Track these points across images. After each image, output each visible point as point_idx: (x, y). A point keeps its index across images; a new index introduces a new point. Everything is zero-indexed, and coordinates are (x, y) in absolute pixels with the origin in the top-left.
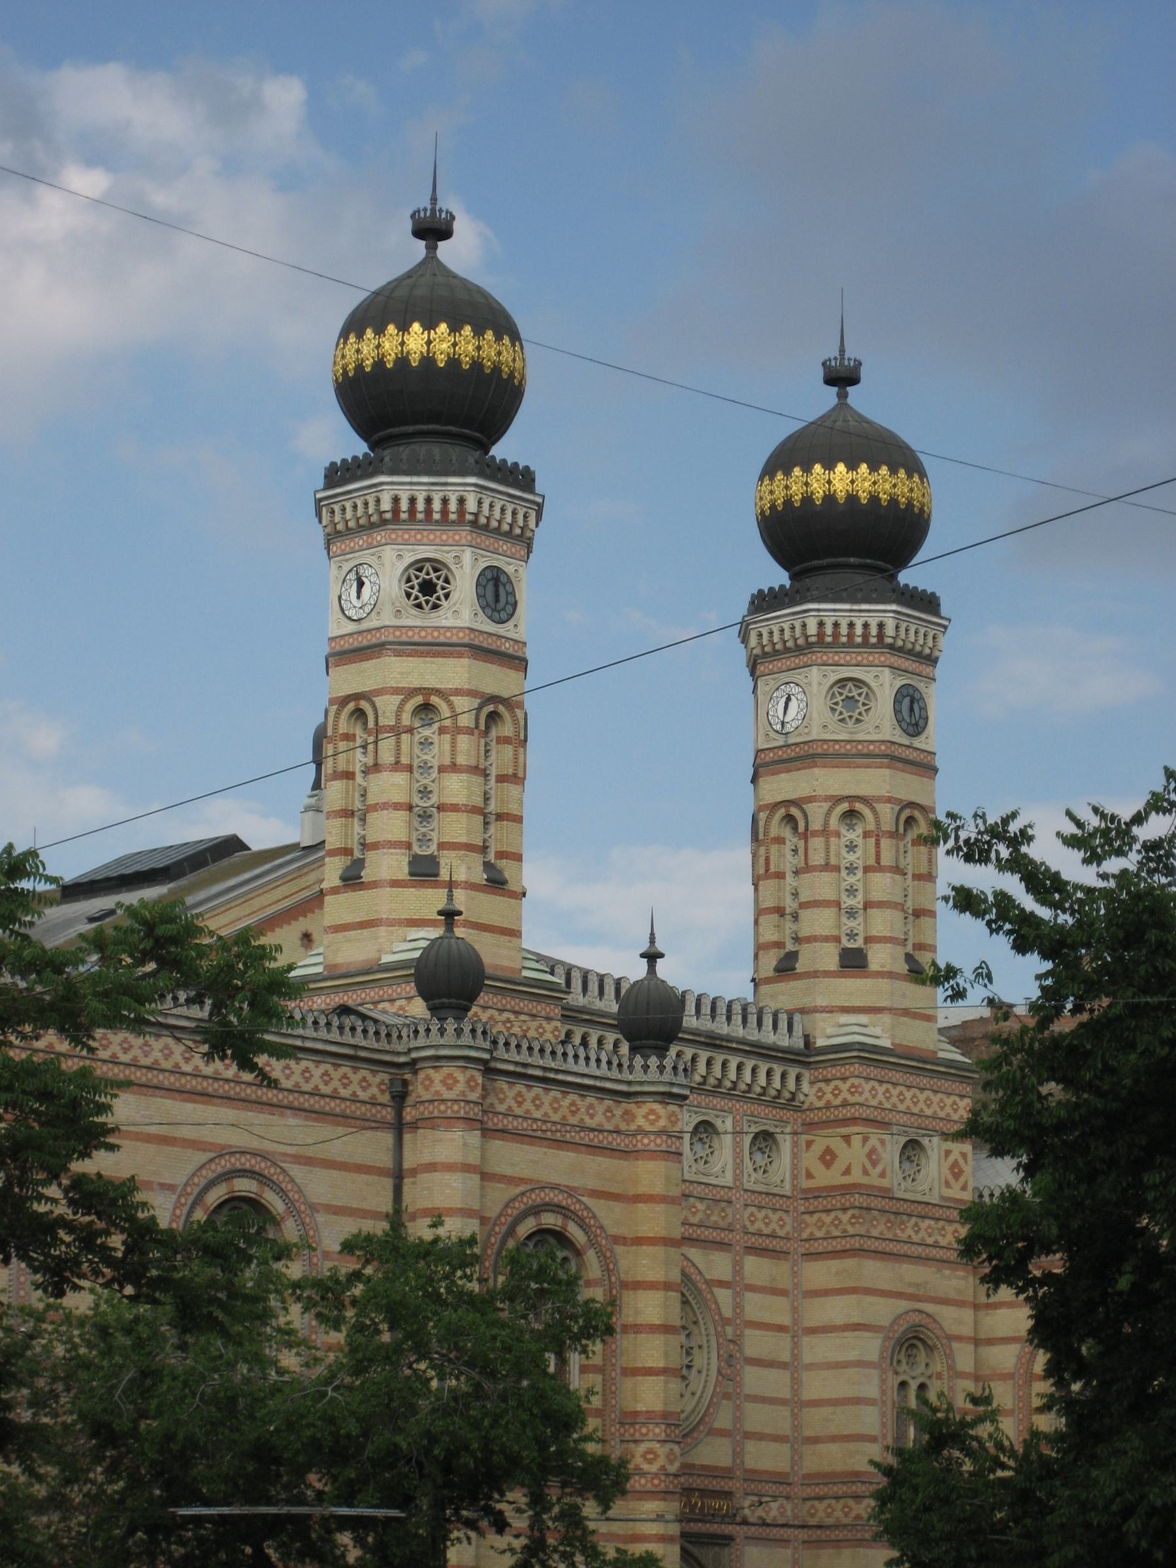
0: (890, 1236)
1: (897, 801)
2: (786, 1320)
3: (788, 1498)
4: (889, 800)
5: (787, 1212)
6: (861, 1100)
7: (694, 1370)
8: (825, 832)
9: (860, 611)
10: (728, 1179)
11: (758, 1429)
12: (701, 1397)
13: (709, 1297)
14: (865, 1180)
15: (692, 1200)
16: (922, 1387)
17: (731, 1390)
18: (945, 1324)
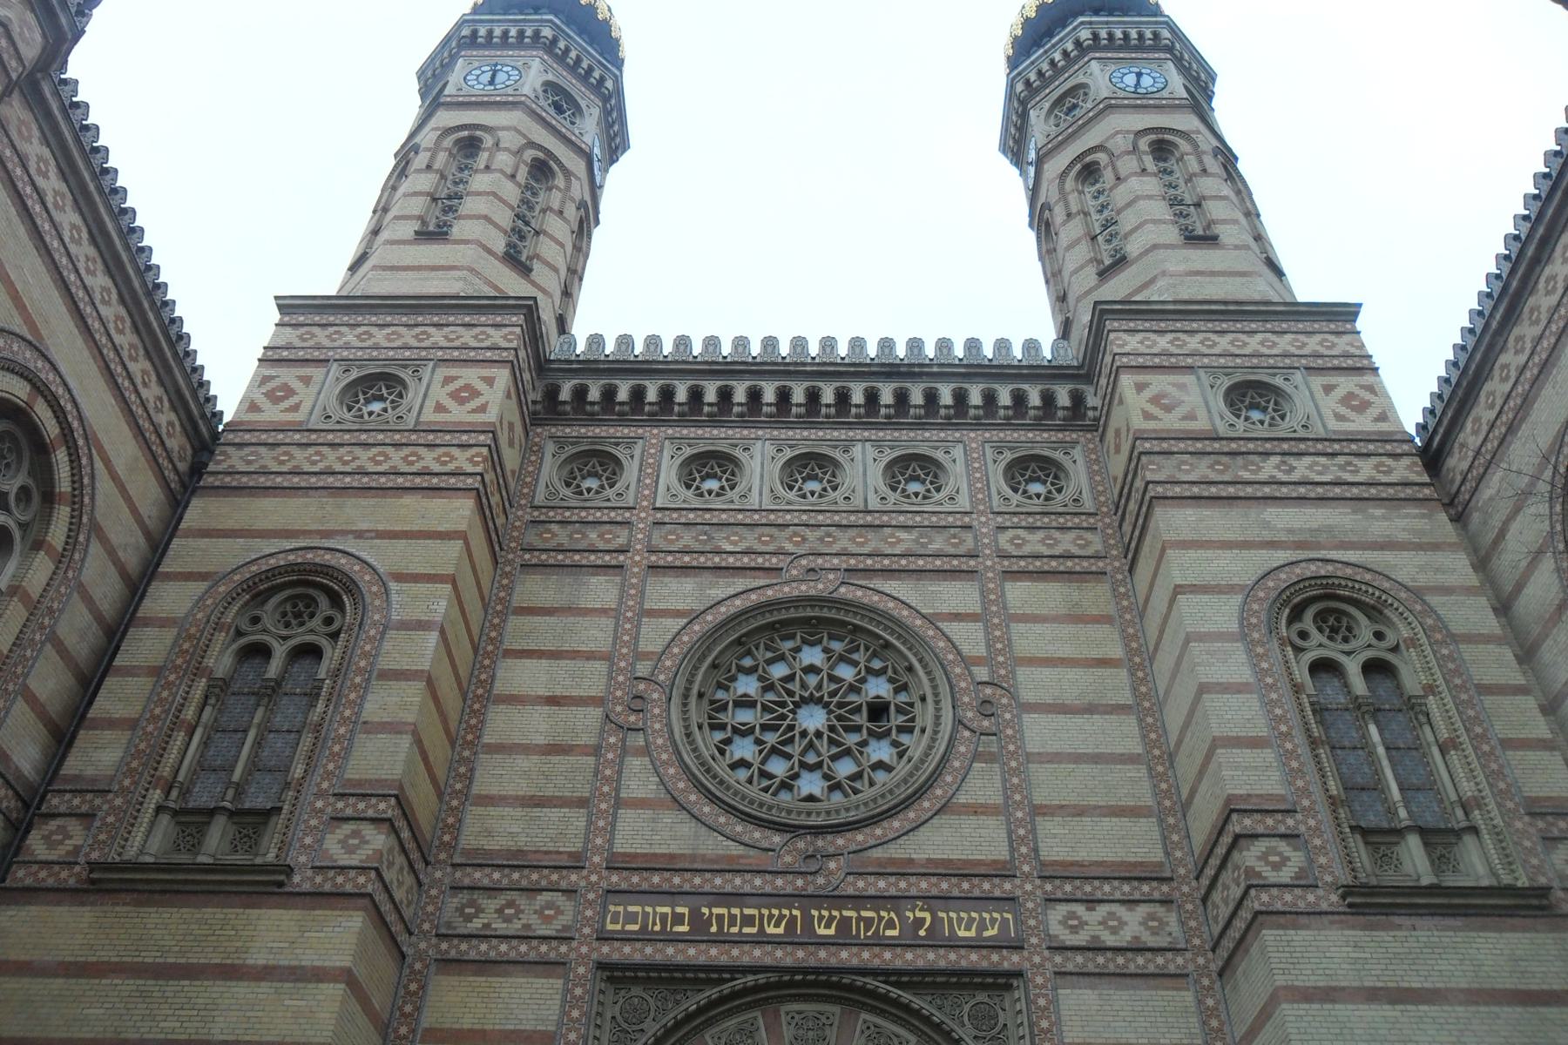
0: (1226, 478)
1: (1128, 132)
2: (1117, 652)
3: (1166, 902)
4: (1117, 133)
5: (1092, 529)
6: (1127, 349)
7: (917, 730)
8: (1063, 195)
9: (1053, 46)
10: (964, 502)
11: (1072, 799)
12: (922, 761)
13: (931, 633)
14: (1151, 425)
15: (888, 531)
16: (1376, 668)
17: (994, 749)
18: (1401, 576)
